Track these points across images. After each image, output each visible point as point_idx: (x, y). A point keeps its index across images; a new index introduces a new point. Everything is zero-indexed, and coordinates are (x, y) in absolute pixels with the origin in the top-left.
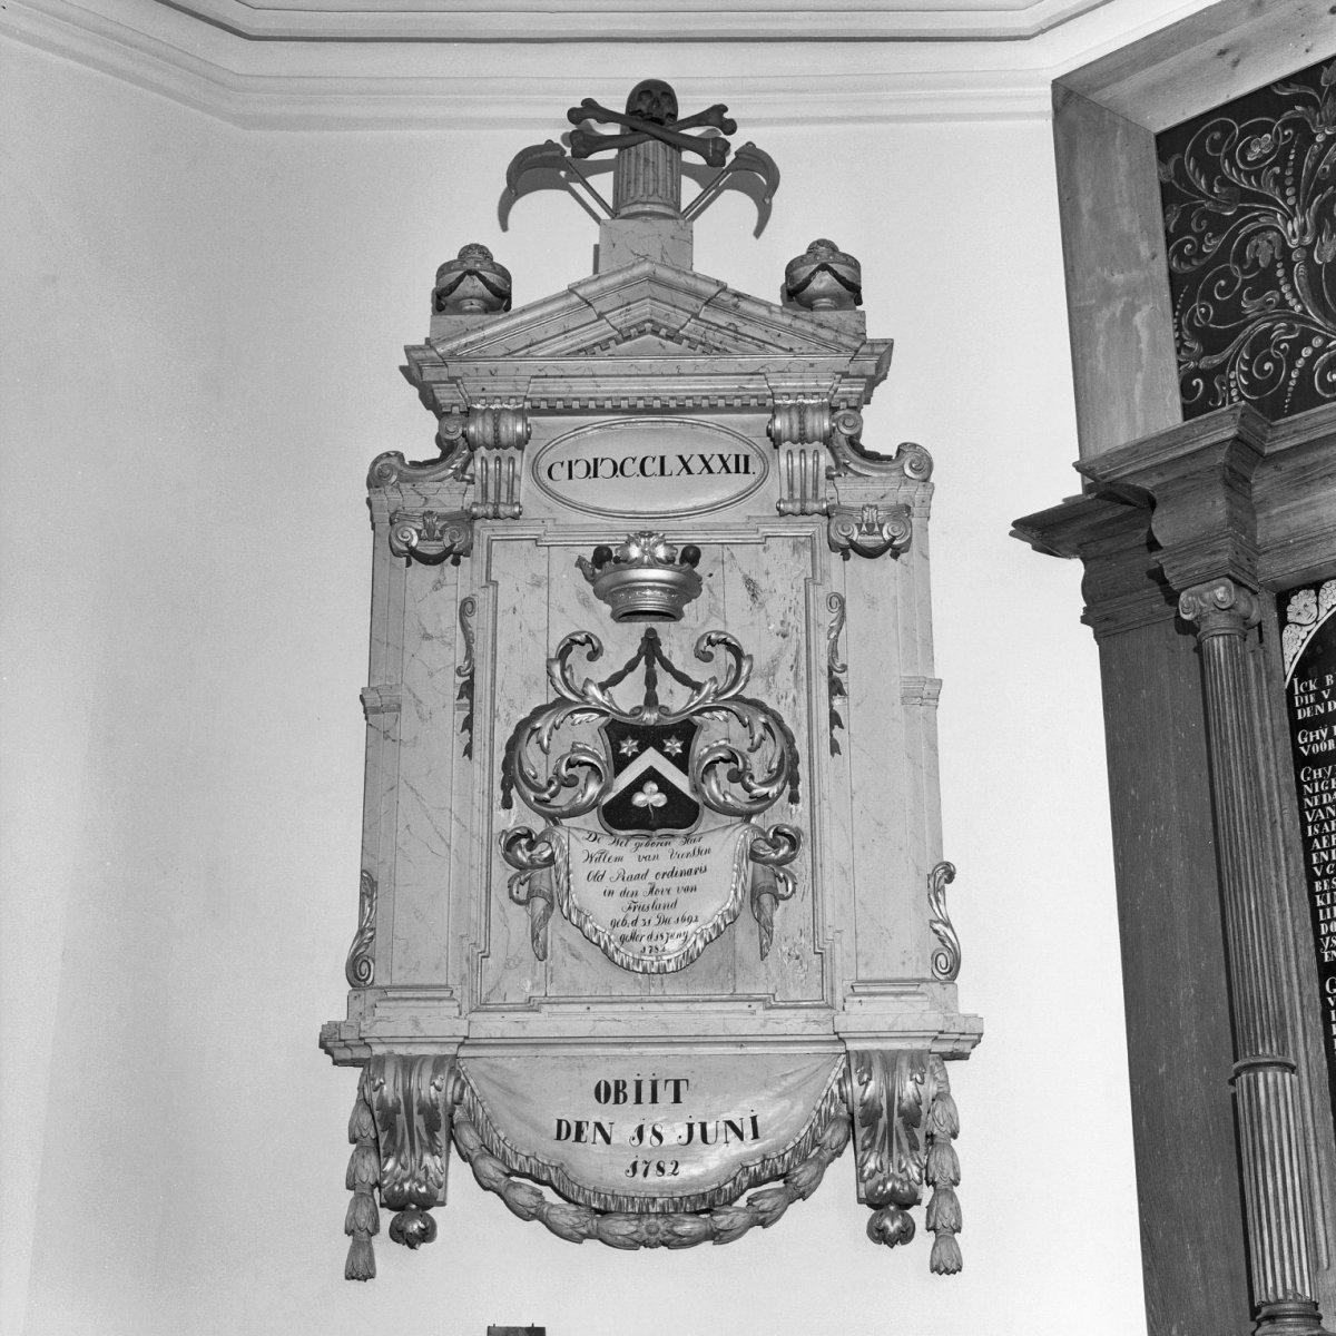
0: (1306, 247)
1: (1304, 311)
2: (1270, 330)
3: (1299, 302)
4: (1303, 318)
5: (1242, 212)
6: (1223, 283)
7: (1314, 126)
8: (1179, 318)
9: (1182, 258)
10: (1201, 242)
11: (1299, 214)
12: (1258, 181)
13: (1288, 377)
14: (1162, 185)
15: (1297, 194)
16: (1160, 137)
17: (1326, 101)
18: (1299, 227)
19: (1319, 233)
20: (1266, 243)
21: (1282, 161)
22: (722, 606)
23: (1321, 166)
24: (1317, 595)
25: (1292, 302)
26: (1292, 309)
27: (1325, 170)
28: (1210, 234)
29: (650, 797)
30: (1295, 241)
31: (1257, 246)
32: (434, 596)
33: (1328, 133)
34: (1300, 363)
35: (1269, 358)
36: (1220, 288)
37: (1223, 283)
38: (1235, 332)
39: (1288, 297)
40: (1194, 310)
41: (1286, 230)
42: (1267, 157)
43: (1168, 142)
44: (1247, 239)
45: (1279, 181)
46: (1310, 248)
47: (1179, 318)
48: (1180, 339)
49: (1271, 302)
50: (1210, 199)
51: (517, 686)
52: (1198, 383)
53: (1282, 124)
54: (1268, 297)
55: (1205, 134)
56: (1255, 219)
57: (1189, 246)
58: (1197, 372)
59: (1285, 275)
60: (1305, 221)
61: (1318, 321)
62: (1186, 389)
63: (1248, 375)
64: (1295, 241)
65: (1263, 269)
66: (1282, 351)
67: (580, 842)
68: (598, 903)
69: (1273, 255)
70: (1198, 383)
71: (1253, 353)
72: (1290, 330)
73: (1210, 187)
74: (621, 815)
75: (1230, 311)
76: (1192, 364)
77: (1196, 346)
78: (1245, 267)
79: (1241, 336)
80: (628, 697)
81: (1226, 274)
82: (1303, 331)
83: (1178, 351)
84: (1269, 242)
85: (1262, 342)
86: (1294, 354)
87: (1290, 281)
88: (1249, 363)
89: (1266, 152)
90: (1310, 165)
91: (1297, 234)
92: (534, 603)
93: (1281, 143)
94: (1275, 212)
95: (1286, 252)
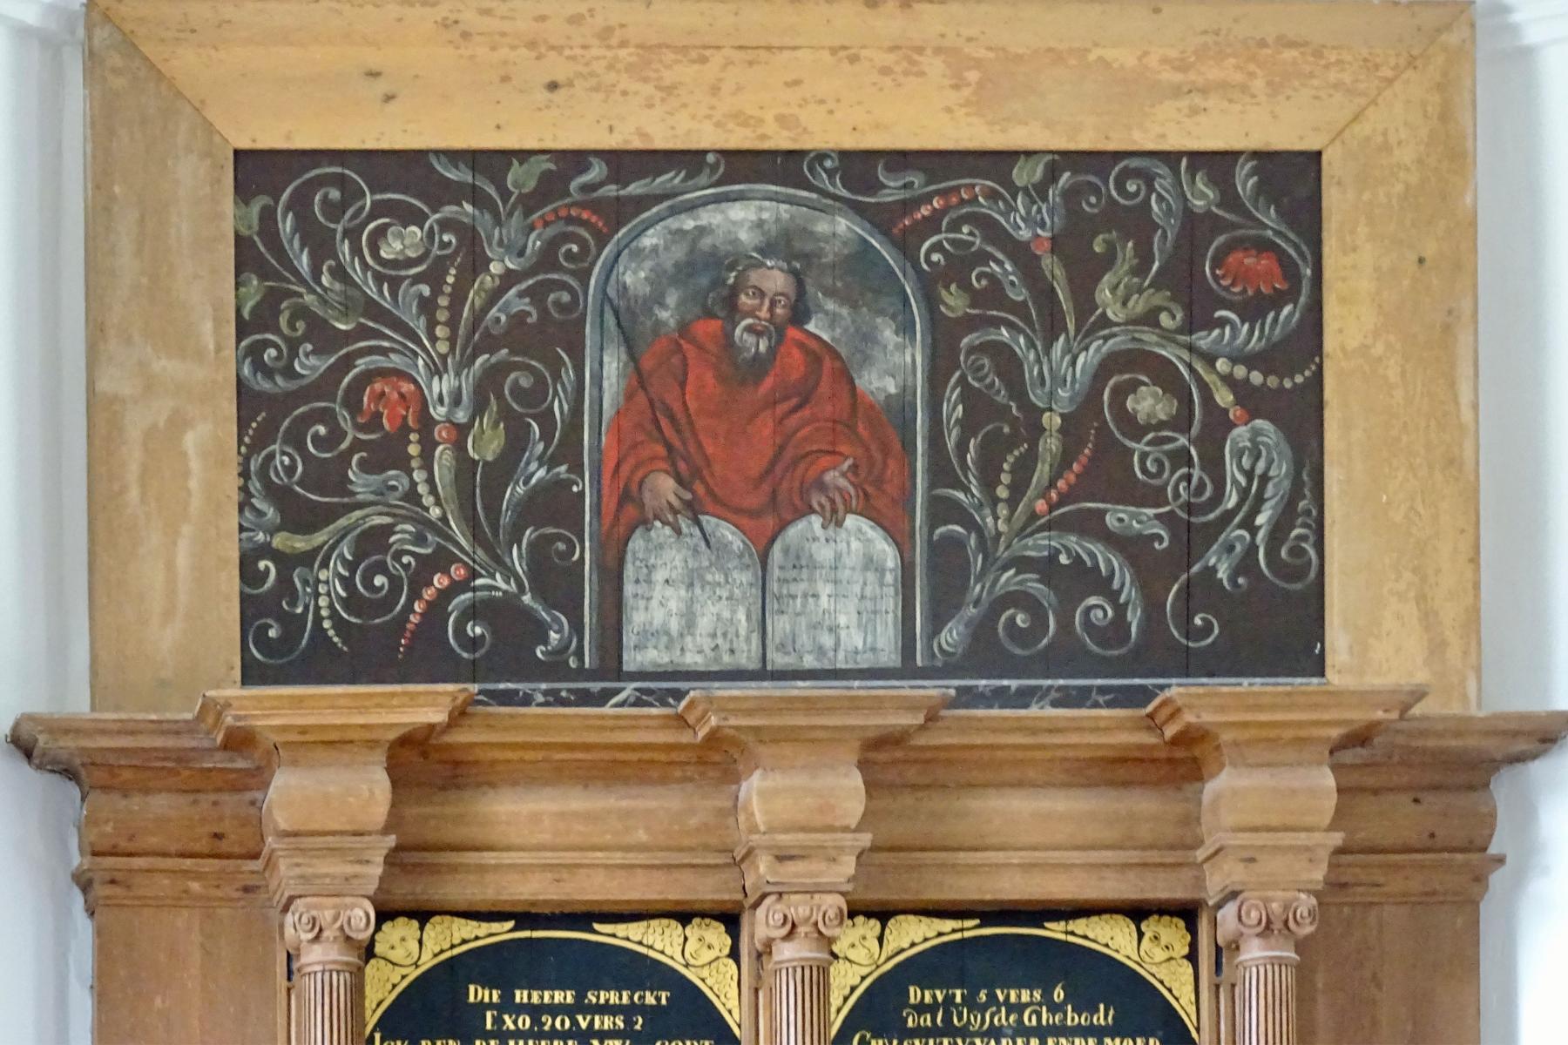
0: (457, 426)
1: (444, 519)
2: (388, 530)
3: (438, 503)
4: (441, 527)
5: (363, 332)
6: (322, 430)
7: (490, 245)
8: (247, 459)
9: (259, 366)
10: (294, 354)
11: (452, 374)
12: (394, 294)
13: (409, 608)
14: (240, 240)
15: (452, 340)
16: (241, 156)
17: (510, 214)
18: (450, 393)
19: (479, 409)
20: (396, 396)
21: (434, 278)
23: (493, 312)
24: (422, 929)
25: (428, 500)
26: (427, 509)
27: (498, 320)
28: (309, 347)
30: (442, 410)
31: (383, 394)
33: (511, 266)
34: (428, 594)
35: (382, 568)
36: (316, 437)
37: (322, 430)
38: (328, 515)
39: (422, 489)
40: (271, 456)
41: (430, 388)
42: (411, 263)
43: (256, 170)
44: (368, 376)
45: (427, 307)
46: (462, 430)
47: (247, 459)
48: (244, 489)
49: (394, 488)
50: (314, 292)
52: (267, 568)
53: (438, 222)
54: (391, 478)
55: (321, 181)
56: (384, 352)
57: (273, 352)
58: (266, 551)
59: (420, 456)
60: (460, 387)
61: (463, 542)
62: (248, 573)
63: (348, 583)
64: (442, 410)
65: (387, 433)
66: (403, 565)
69: (405, 418)
70: (267, 568)
71: (359, 555)
72: (420, 539)
73: (316, 273)
75: (330, 478)
76: (261, 537)
77: (271, 512)
78: (360, 420)
79: (343, 522)
81: (326, 416)
82: (439, 547)
83: (241, 510)
84: (402, 396)
85: (373, 541)
86: (420, 580)
87: (428, 466)
88: (352, 567)
89: (412, 254)
90: (478, 303)
91: (446, 400)
93: (436, 251)
94: (416, 354)
95: (426, 422)
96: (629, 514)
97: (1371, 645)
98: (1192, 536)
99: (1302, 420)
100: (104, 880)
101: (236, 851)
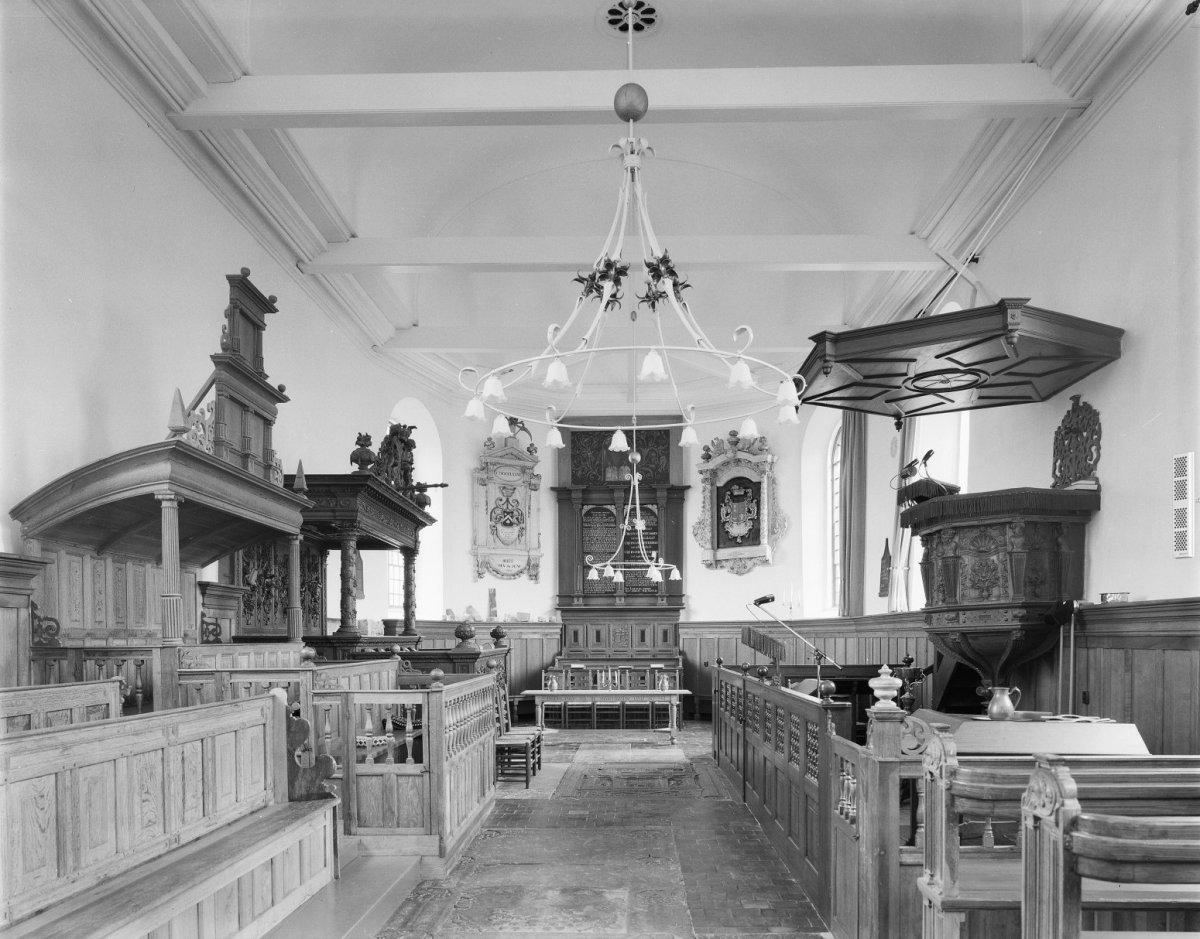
22: (517, 495)
29: (508, 522)
32: (482, 489)
51: (492, 506)
67: (500, 527)
68: (501, 535)
74: (505, 524)
80: (505, 507)
92: (495, 492)
96: (607, 466)
97: (674, 480)
98: (657, 468)
99: (668, 456)
100: (560, 501)
101: (570, 499)
